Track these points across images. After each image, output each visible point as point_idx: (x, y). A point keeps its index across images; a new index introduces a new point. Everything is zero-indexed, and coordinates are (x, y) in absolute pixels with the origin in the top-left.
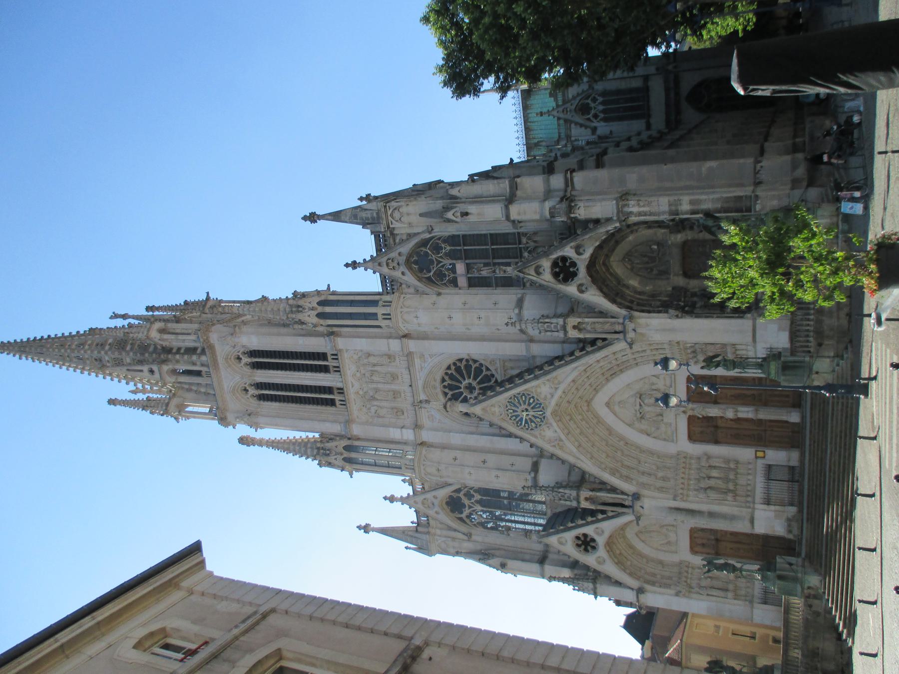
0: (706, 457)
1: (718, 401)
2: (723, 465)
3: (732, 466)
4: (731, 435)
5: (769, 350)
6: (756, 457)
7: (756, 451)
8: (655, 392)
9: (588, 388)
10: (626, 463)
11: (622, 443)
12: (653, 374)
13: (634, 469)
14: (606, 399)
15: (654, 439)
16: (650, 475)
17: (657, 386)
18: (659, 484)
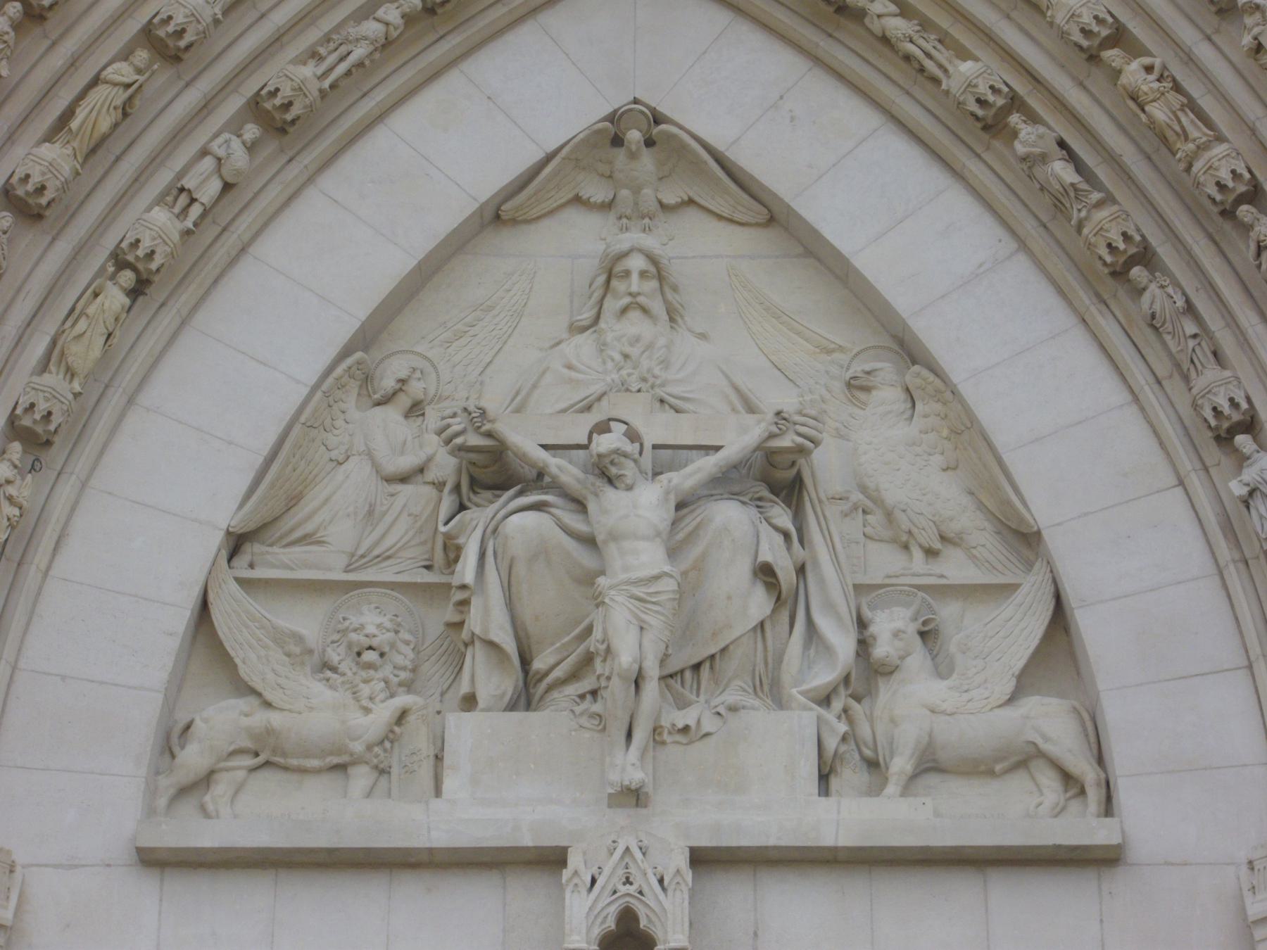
8: (843, 643)
12: (1085, 621)
15: (181, 617)
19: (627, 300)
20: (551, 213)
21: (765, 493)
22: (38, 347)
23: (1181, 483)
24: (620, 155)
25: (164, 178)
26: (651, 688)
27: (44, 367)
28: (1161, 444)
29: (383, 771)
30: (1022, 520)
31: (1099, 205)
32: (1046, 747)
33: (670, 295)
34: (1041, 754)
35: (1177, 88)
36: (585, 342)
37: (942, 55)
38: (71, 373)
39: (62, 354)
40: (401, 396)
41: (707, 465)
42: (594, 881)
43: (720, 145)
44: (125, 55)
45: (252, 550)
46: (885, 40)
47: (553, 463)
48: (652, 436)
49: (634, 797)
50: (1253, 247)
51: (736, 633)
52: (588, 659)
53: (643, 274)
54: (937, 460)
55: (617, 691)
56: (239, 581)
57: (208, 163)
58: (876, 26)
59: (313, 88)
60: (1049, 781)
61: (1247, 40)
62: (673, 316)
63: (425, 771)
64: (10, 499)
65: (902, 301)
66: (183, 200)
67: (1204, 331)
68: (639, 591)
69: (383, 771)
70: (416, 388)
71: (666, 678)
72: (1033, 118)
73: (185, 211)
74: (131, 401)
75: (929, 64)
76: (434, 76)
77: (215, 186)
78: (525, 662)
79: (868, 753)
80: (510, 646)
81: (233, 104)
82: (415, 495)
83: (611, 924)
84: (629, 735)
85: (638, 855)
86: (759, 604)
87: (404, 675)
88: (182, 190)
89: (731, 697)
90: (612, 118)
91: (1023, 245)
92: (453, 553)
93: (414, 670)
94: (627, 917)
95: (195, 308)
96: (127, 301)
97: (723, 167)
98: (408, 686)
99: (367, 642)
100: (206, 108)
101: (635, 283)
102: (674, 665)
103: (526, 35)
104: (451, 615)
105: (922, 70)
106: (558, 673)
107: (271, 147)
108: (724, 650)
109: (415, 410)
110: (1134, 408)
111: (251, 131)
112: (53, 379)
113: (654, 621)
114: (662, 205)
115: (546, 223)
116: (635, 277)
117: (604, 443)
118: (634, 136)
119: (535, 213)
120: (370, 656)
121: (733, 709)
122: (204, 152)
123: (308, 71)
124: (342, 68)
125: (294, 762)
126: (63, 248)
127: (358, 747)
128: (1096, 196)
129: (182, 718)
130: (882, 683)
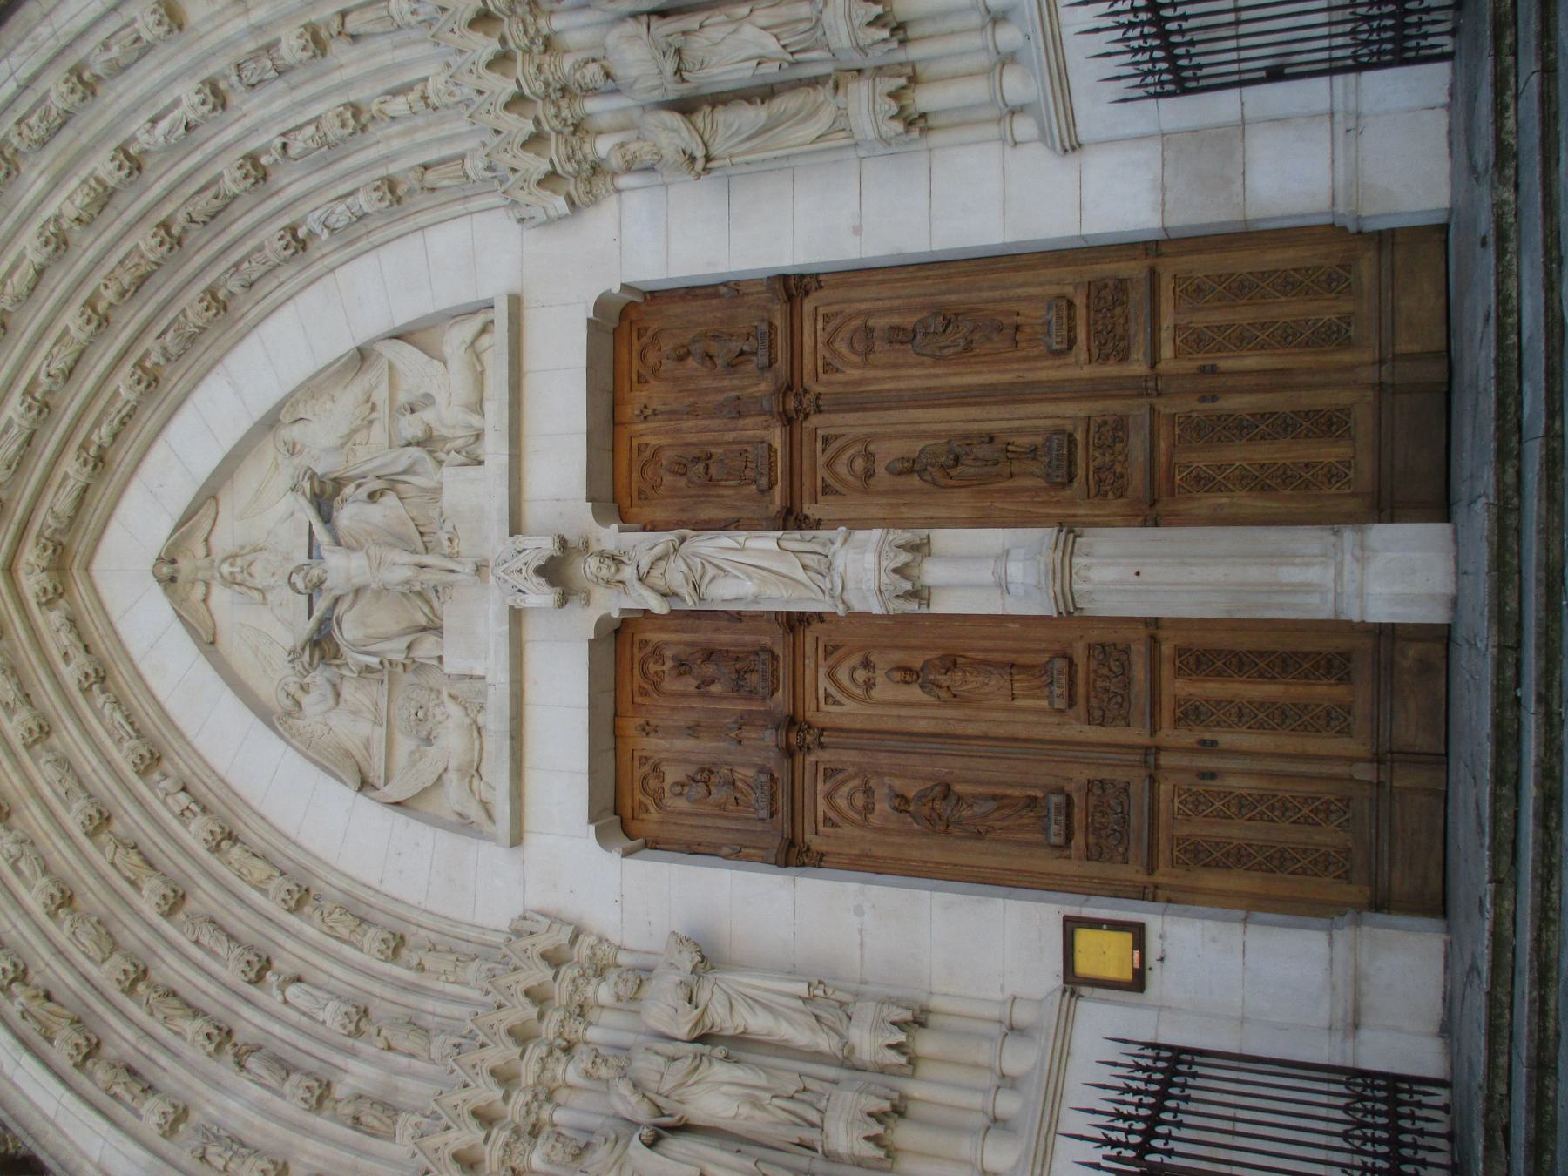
0: (687, 959)
1: (809, 509)
2: (800, 1034)
3: (868, 1042)
4: (901, 802)
6: (1074, 981)
7: (1071, 925)
10: (170, 969)
11: (194, 834)
12: (402, 319)
13: (197, 1012)
14: (158, 533)
15: (398, 818)
16: (286, 1068)
17: (428, 415)
19: (246, 575)
20: (211, 616)
21: (339, 498)
22: (255, 896)
23: (332, 270)
24: (181, 579)
25: (175, 825)
26: (426, 559)
27: (264, 892)
28: (312, 282)
30: (352, 358)
31: (185, 317)
32: (468, 343)
33: (246, 551)
34: (473, 343)
36: (270, 597)
37: (119, 405)
38: (270, 877)
39: (261, 882)
40: (297, 696)
41: (318, 528)
42: (520, 591)
43: (172, 525)
44: (101, 849)
45: (372, 778)
46: (115, 436)
47: (317, 614)
49: (480, 569)
50: (192, 225)
51: (403, 512)
53: (232, 565)
54: (329, 405)
55: (426, 576)
56: (385, 784)
57: (170, 800)
58: (106, 440)
60: (485, 341)
61: (76, 227)
63: (478, 685)
64: (330, 914)
65: (245, 425)
66: (187, 813)
67: (247, 258)
68: (375, 565)
69: (482, 707)
70: (293, 689)
72: (147, 354)
73: (194, 814)
74: (294, 843)
75: (124, 412)
76: (140, 677)
77: (182, 797)
78: (424, 629)
79: (472, 440)
80: (409, 638)
81: (140, 787)
83: (542, 581)
84: (452, 571)
85: (506, 565)
86: (390, 500)
87: (433, 696)
88: (182, 814)
89: (435, 514)
91: (219, 360)
92: (368, 669)
93: (432, 690)
94: (540, 571)
95: (250, 807)
96: (239, 845)
97: (186, 522)
98: (439, 692)
99: (413, 717)
100: (140, 802)
102: (420, 547)
105: (129, 416)
106: (427, 610)
108: (413, 520)
110: (297, 298)
111: (156, 776)
112: (271, 887)
114: (208, 555)
115: (216, 618)
116: (234, 569)
119: (210, 623)
120: (420, 714)
121: (441, 514)
122: (164, 803)
124: (128, 727)
125: (476, 756)
126: (204, 882)
127: (467, 721)
128: (182, 319)
129: (454, 818)
130: (435, 433)
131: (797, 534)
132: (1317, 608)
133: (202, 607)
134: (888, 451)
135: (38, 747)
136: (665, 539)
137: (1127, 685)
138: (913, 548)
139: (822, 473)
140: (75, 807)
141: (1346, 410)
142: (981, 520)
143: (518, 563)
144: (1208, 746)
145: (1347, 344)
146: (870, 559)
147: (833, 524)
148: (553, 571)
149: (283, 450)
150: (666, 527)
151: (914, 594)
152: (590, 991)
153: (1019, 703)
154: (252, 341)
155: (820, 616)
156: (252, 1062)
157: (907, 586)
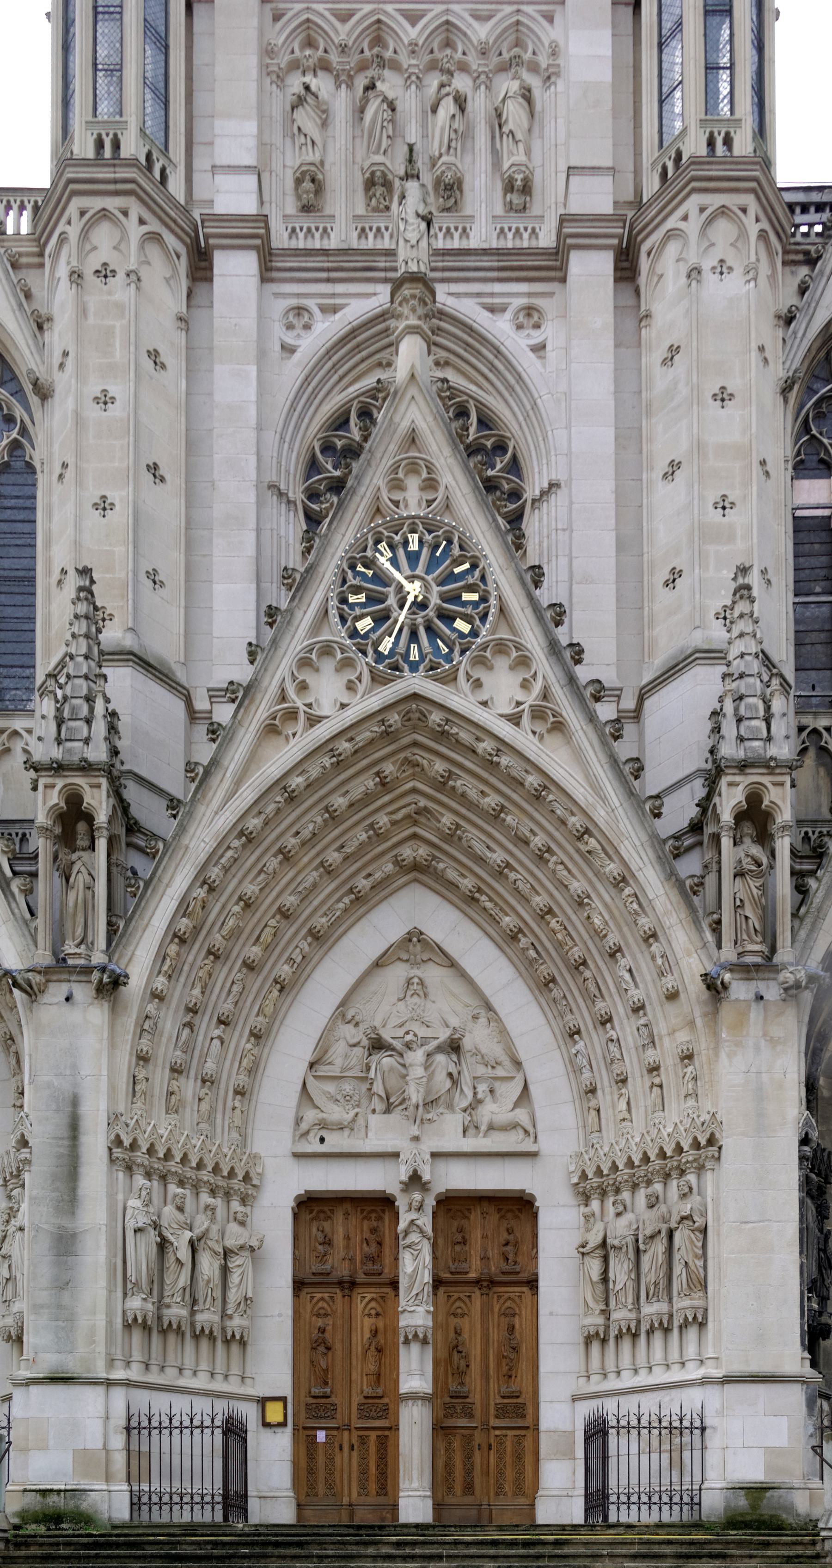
5: (697, 1424)
9: (497, 857)
18: (160, 1076)
29: (352, 1130)
35: (565, 928)
48: (420, 1035)
52: (404, 1100)
59: (326, 926)
62: (426, 995)
71: (425, 1105)
82: (358, 1051)
90: (408, 933)
101: (415, 987)
103: (384, 906)
104: (368, 1086)
107: (315, 944)
109: (357, 1025)
113: (422, 1090)
117: (408, 1038)
118: (415, 939)
123: (324, 920)
131: (431, 1289)
132: (403, 1484)
133: (396, 957)
134: (465, 1323)
135: (322, 870)
136: (429, 1229)
137: (373, 1418)
138: (425, 1337)
139: (456, 1295)
140: (292, 898)
141: (473, 1494)
142: (436, 1363)
143: (419, 1161)
144: (352, 1448)
145: (497, 1494)
146: (420, 1322)
147: (435, 1304)
148: (415, 1180)
149: (475, 1012)
150: (434, 1229)
151: (406, 1337)
152: (235, 1197)
153: (365, 1378)
154: (530, 997)
155: (397, 1295)
156: (187, 1031)
157: (410, 1337)
